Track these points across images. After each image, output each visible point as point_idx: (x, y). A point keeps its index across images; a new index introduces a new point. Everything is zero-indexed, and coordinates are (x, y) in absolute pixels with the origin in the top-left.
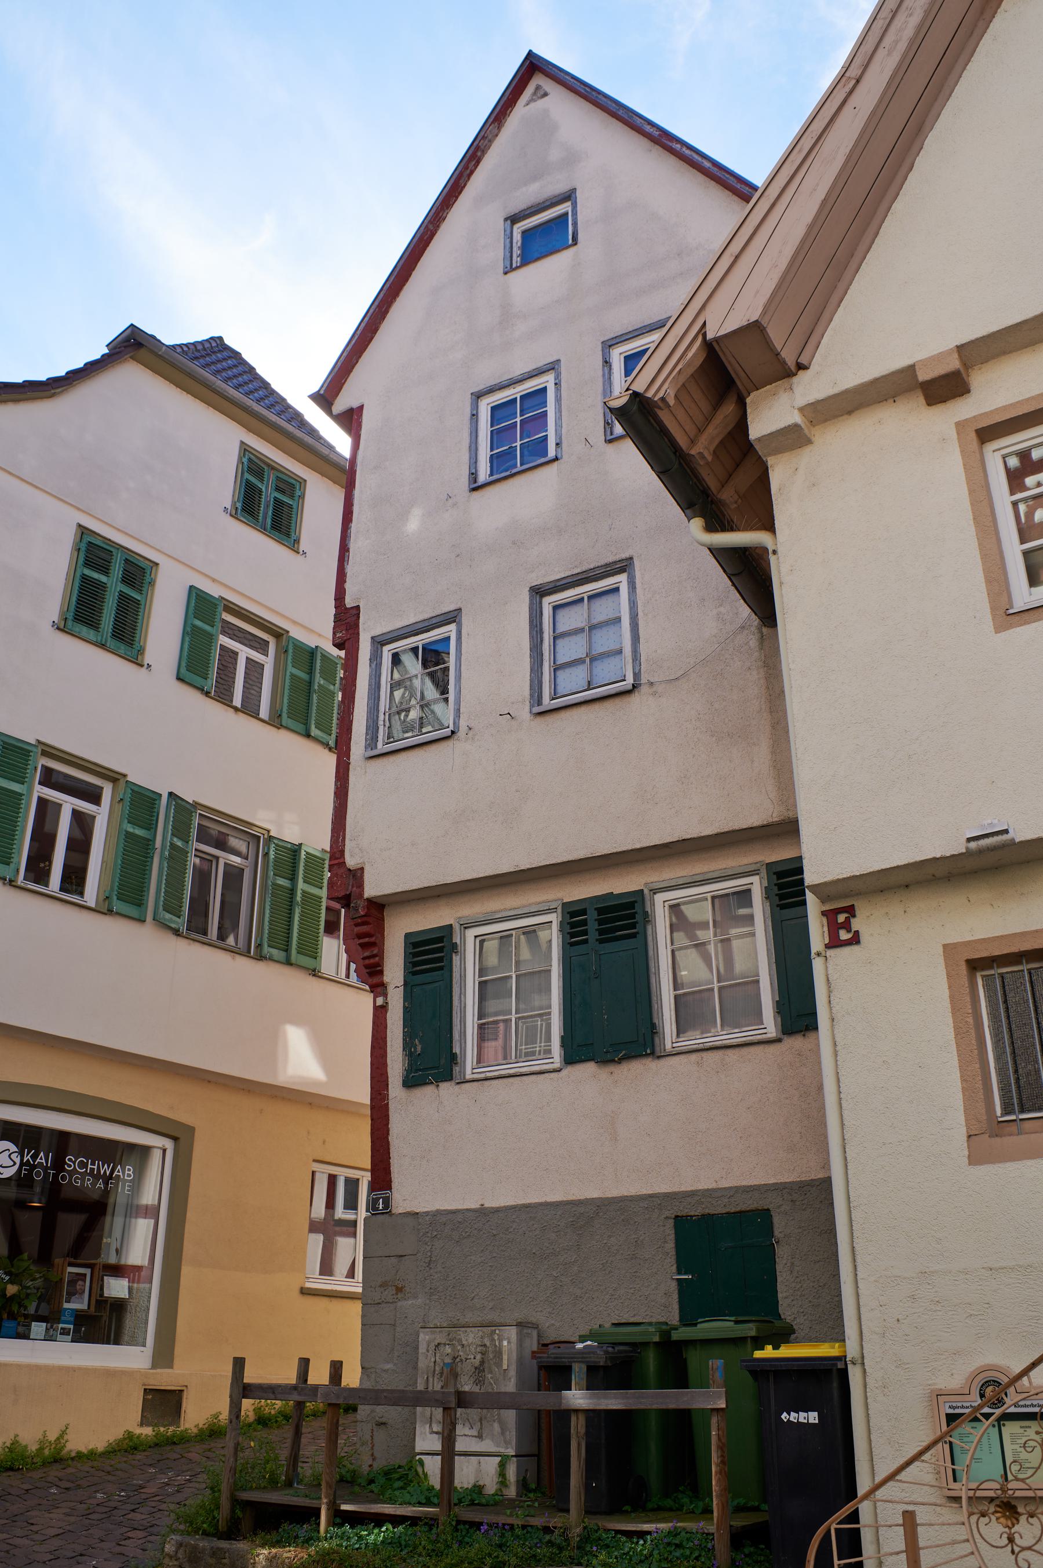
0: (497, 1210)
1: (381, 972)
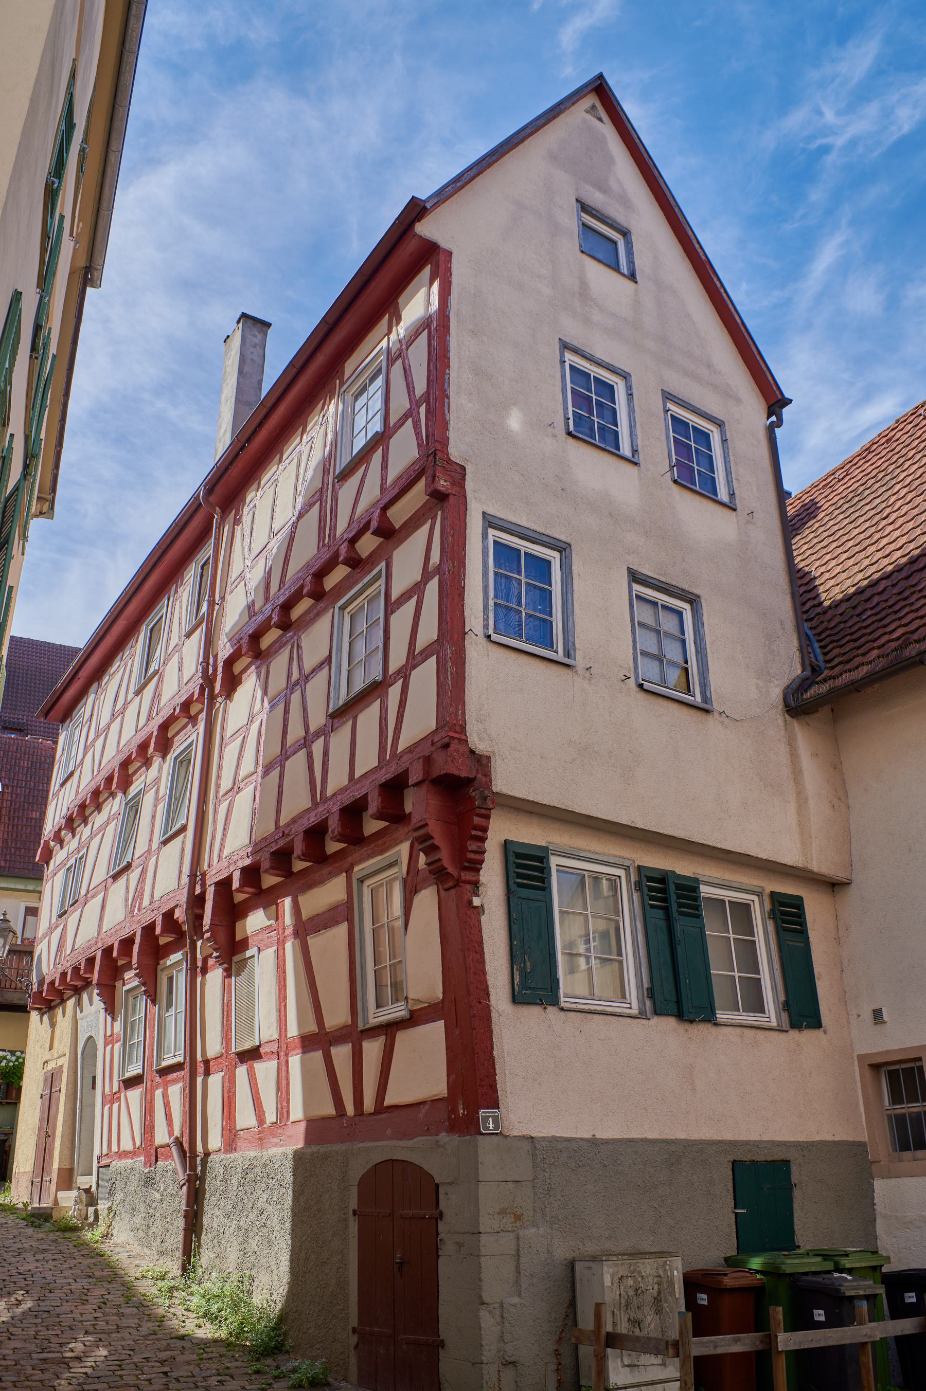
0: (606, 1142)
1: (478, 870)
